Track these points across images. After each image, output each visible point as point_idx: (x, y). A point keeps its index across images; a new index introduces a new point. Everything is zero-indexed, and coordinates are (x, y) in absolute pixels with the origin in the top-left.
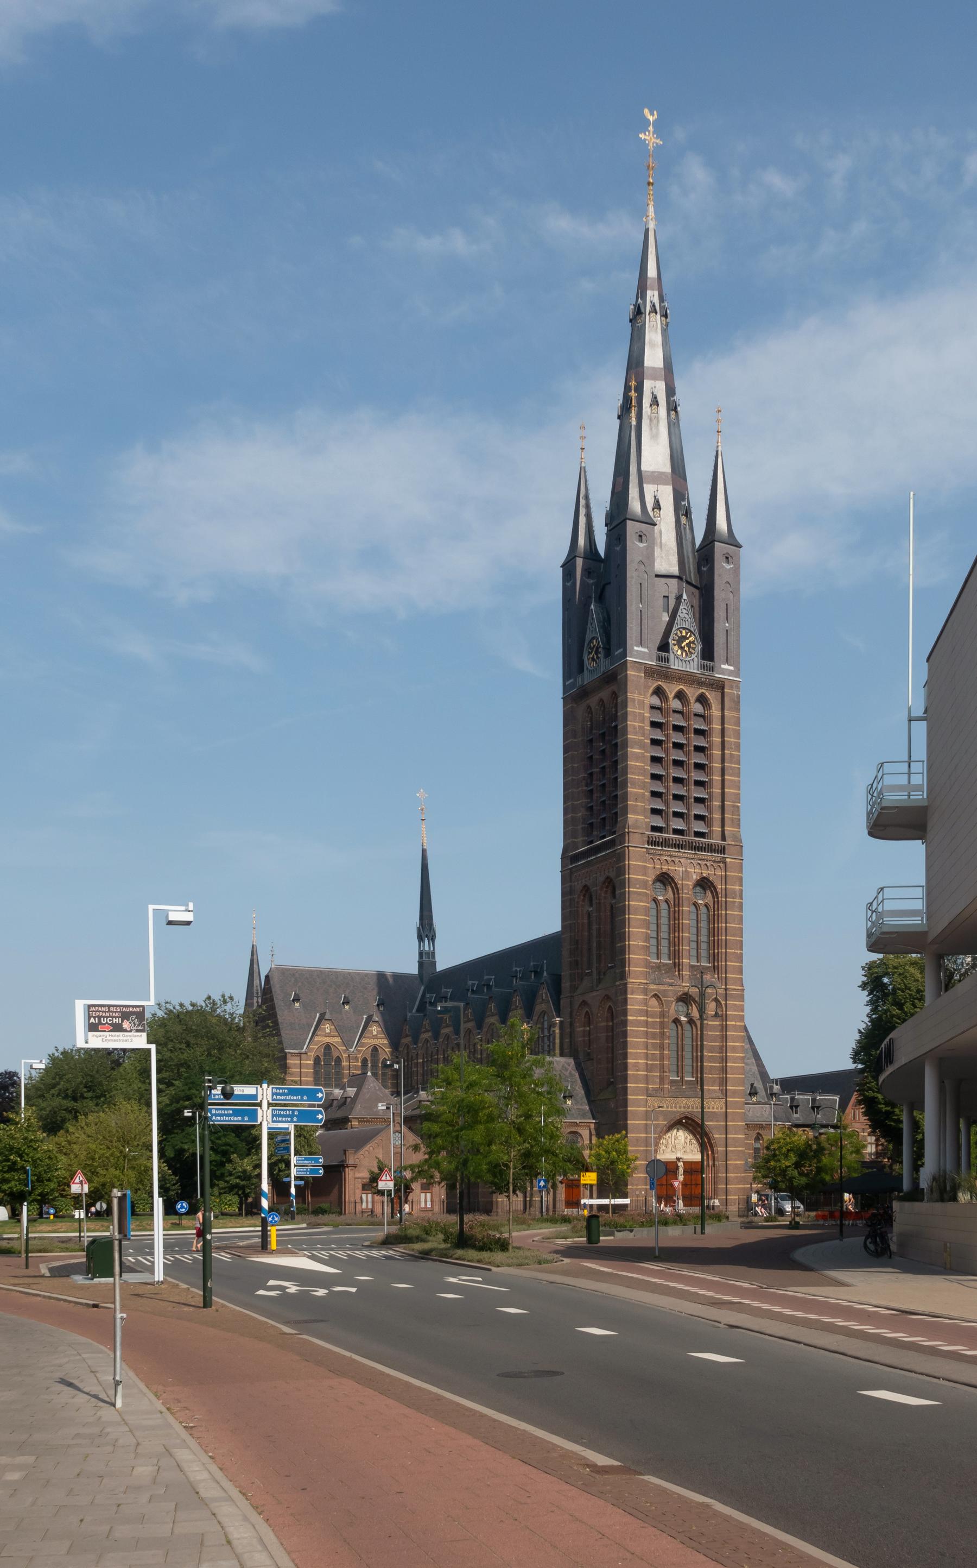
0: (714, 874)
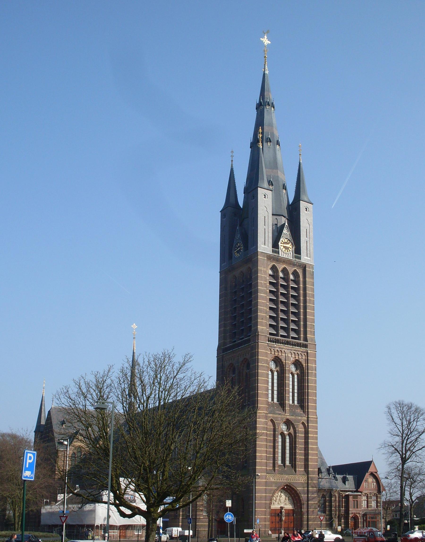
0: (302, 360)
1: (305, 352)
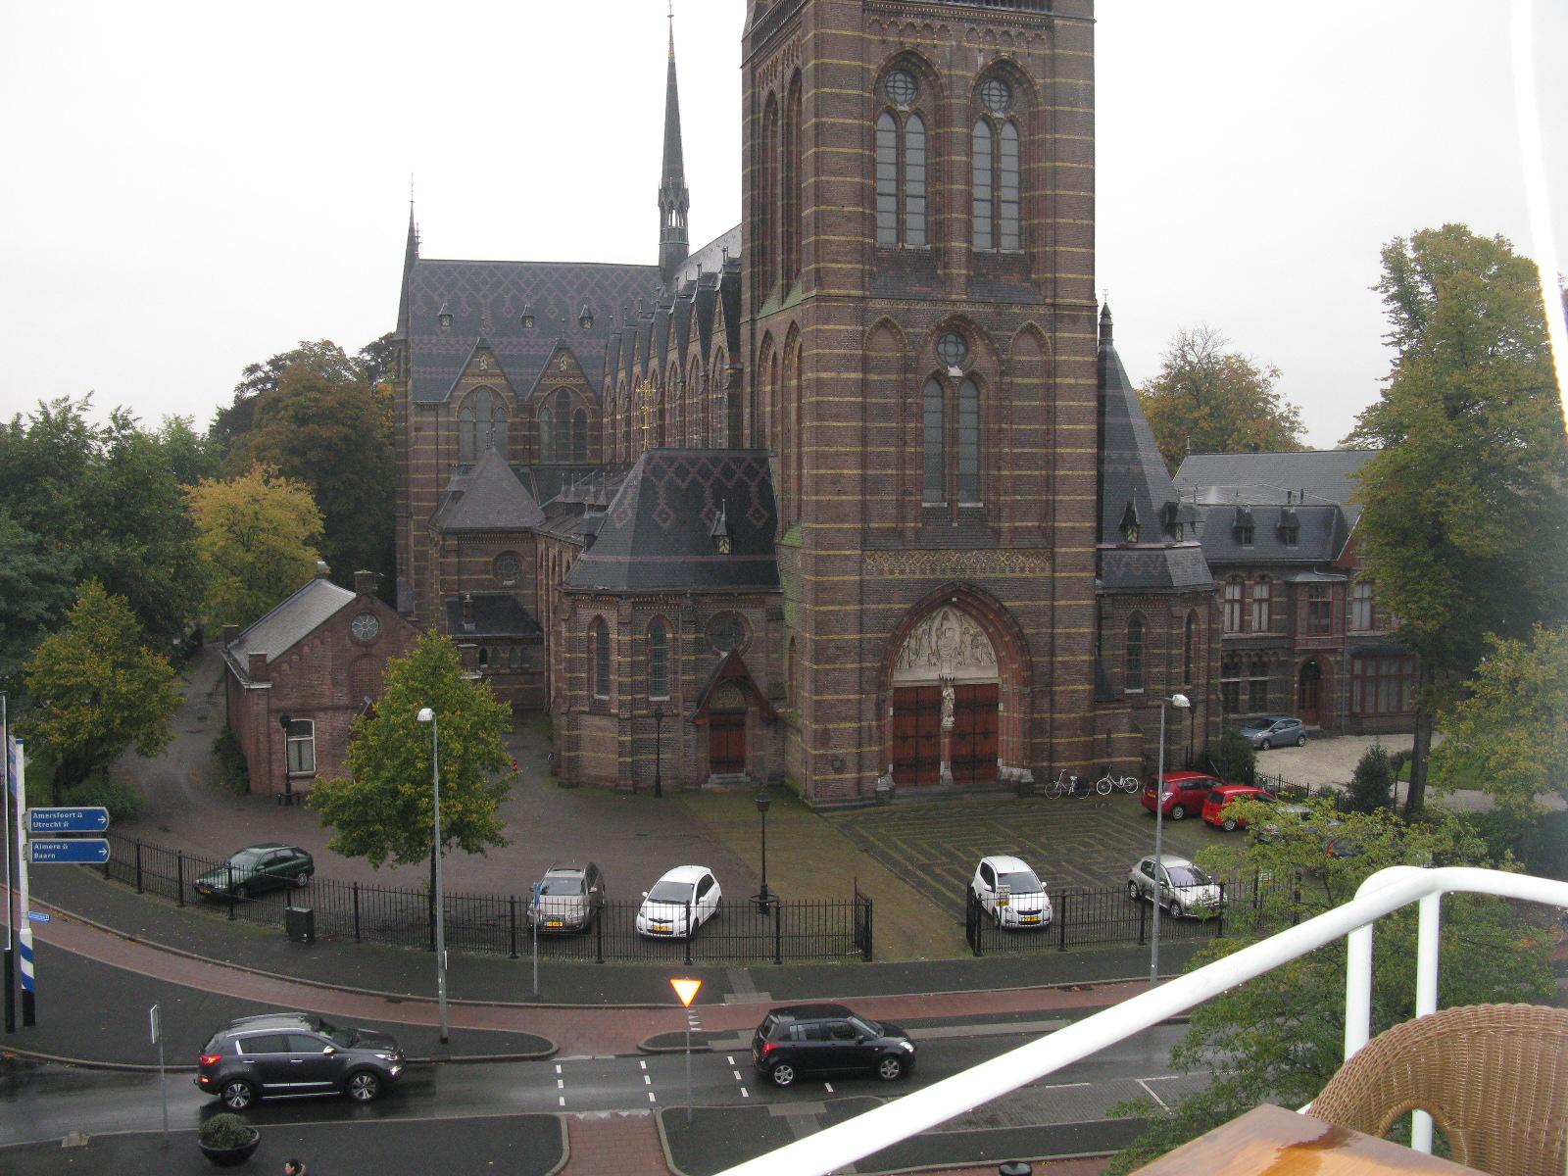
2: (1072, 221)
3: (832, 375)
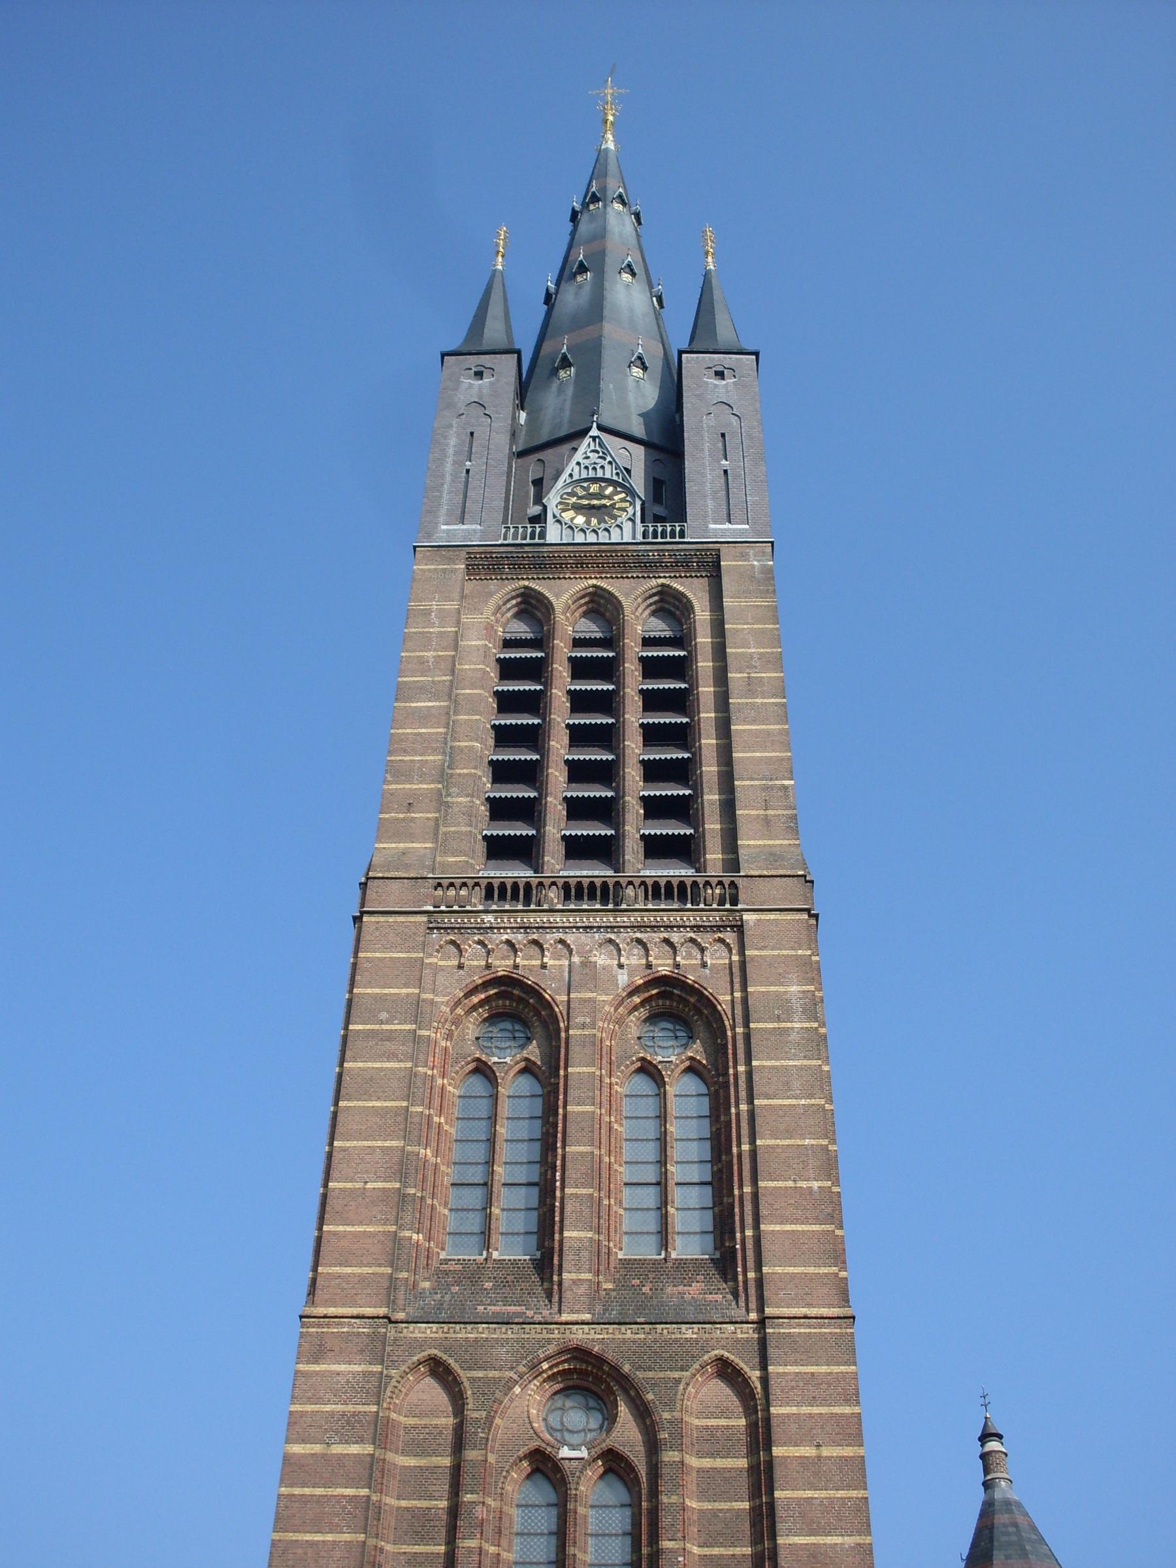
0: (706, 966)
1: (720, 928)
2: (790, 1184)
3: (317, 1448)
